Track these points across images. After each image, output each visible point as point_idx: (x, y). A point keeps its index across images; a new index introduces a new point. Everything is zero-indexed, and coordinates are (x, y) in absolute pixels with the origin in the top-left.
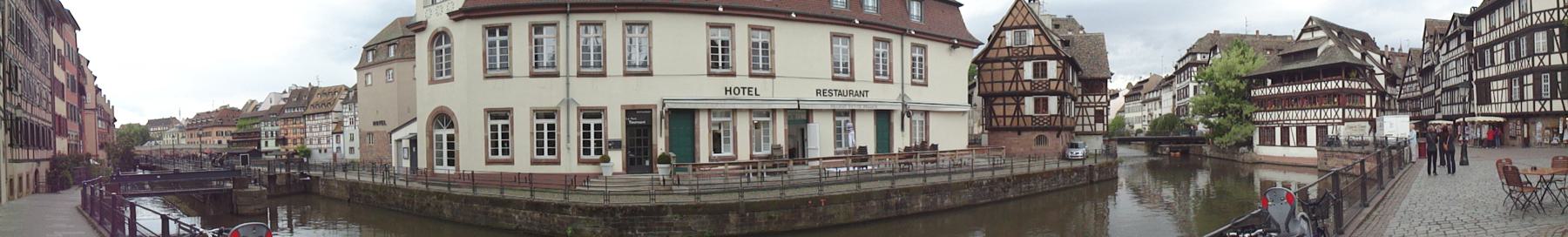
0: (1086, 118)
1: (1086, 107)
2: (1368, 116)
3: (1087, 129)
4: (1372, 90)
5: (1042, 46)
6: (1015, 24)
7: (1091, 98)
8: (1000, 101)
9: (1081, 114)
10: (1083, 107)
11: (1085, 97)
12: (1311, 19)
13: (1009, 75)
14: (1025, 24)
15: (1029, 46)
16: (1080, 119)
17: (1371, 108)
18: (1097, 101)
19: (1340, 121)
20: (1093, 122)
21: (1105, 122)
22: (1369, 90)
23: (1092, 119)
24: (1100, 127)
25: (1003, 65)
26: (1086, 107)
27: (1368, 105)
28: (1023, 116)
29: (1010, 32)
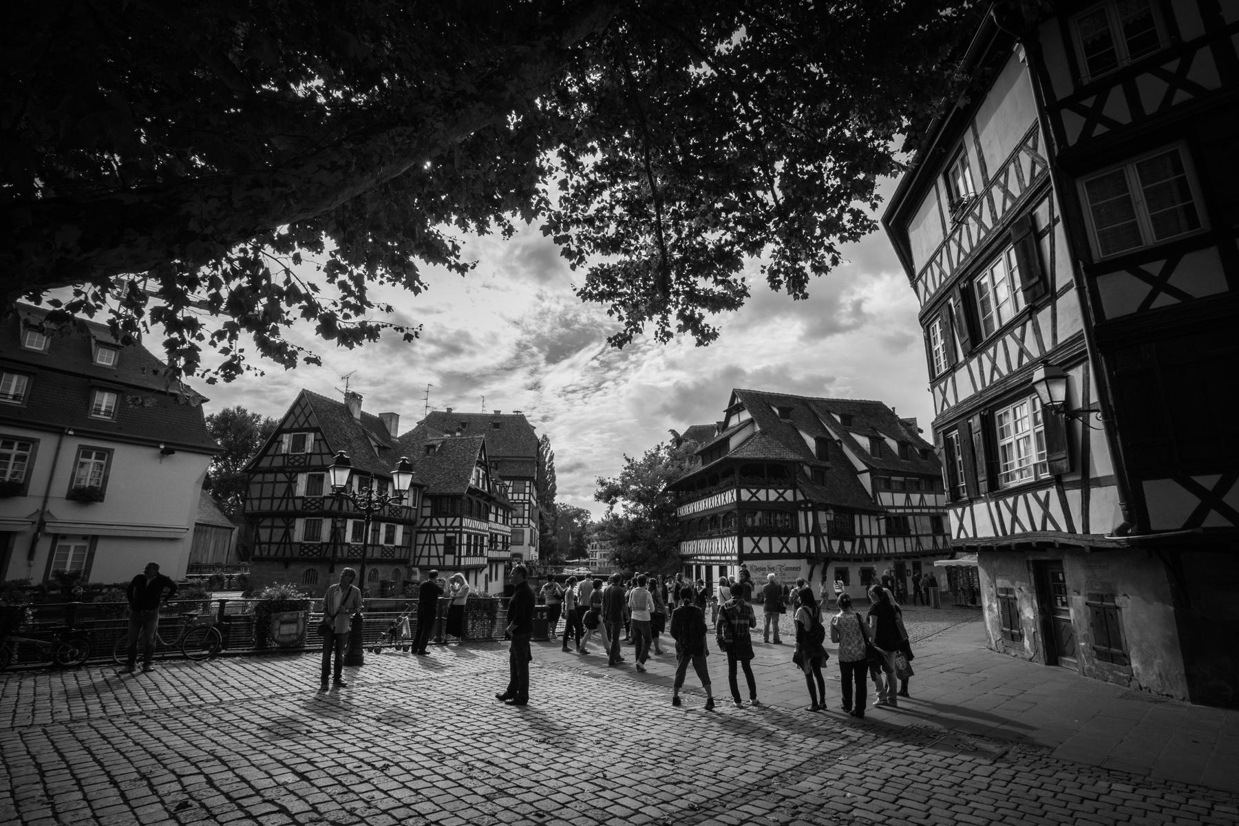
0: (433, 548)
2: (803, 550)
4: (806, 502)
5: (321, 454)
6: (296, 426)
7: (442, 521)
8: (267, 522)
9: (427, 542)
11: (434, 520)
12: (734, 397)
13: (280, 490)
14: (306, 425)
15: (307, 454)
16: (426, 548)
17: (807, 535)
18: (448, 525)
19: (735, 558)
20: (441, 554)
22: (801, 502)
23: (441, 549)
25: (275, 477)
27: (802, 529)
28: (291, 543)
29: (288, 435)
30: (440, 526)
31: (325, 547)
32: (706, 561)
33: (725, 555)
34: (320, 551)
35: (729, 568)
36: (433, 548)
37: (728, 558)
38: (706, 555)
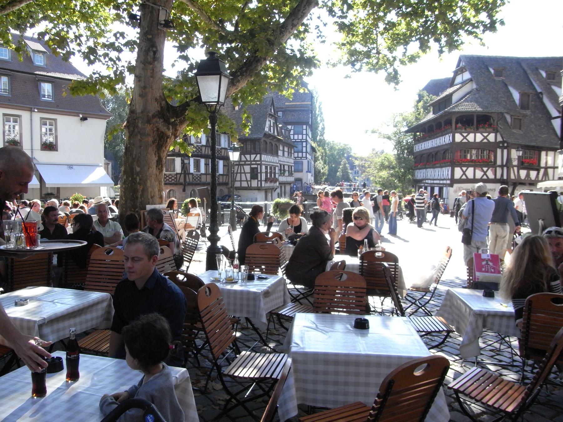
0: (243, 175)
1: (243, 165)
3: (245, 184)
4: (503, 142)
7: (248, 157)
9: (239, 171)
10: (241, 165)
16: (239, 175)
17: (502, 166)
18: (252, 159)
19: (448, 182)
20: (249, 179)
21: (259, 179)
22: (500, 142)
23: (248, 176)
24: (254, 183)
26: (243, 165)
27: (499, 162)
30: (247, 161)
31: (178, 176)
32: (431, 184)
33: (443, 180)
34: (176, 178)
35: (445, 189)
36: (243, 175)
37: (445, 182)
38: (431, 180)
